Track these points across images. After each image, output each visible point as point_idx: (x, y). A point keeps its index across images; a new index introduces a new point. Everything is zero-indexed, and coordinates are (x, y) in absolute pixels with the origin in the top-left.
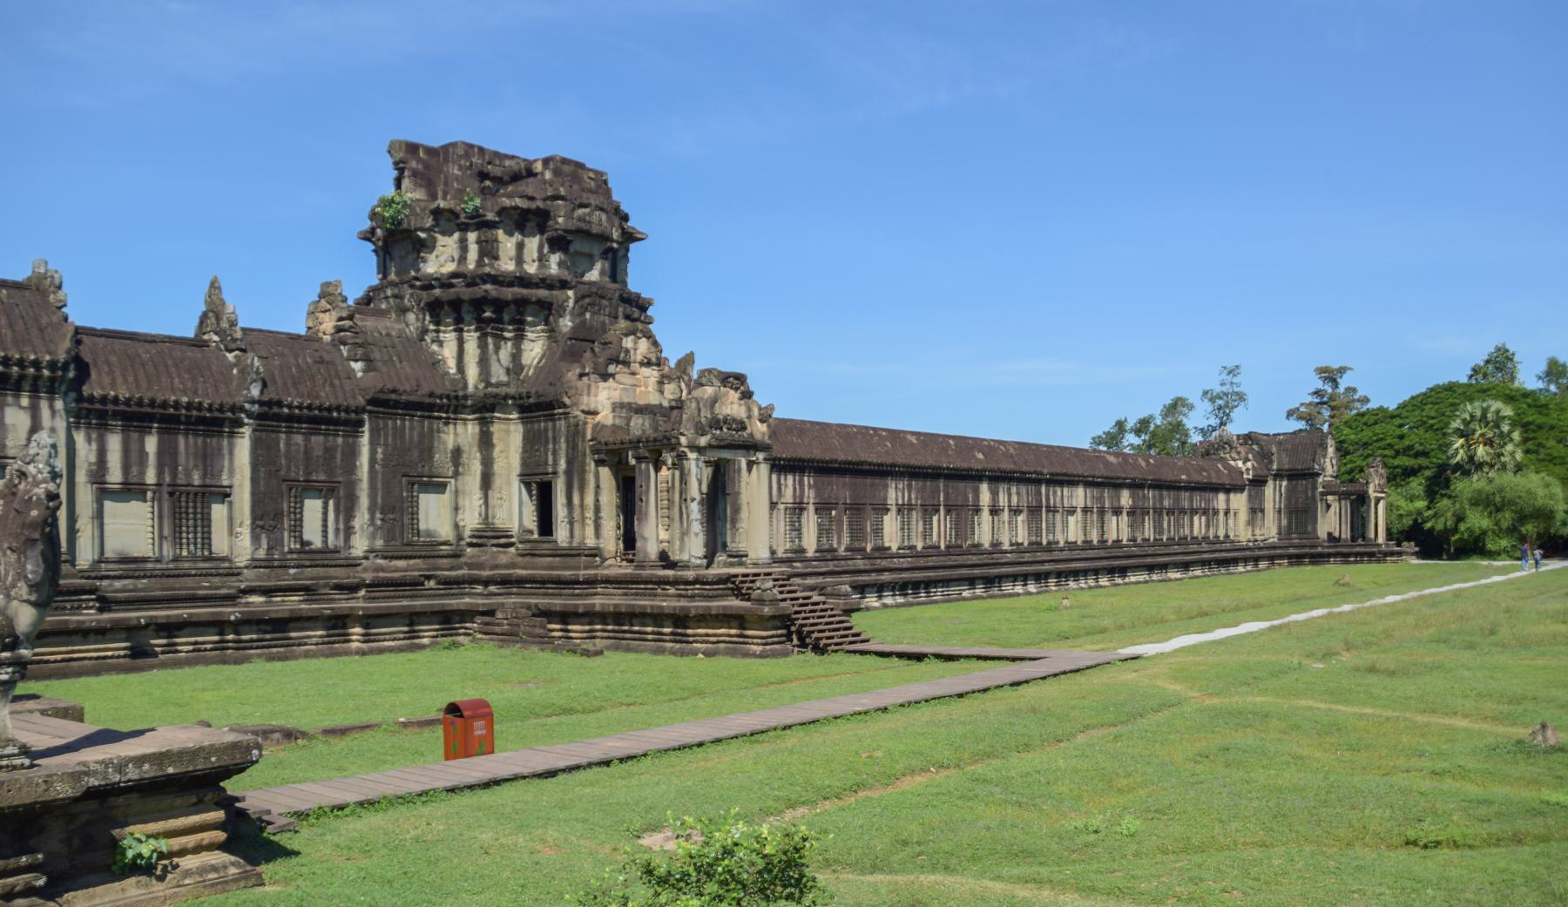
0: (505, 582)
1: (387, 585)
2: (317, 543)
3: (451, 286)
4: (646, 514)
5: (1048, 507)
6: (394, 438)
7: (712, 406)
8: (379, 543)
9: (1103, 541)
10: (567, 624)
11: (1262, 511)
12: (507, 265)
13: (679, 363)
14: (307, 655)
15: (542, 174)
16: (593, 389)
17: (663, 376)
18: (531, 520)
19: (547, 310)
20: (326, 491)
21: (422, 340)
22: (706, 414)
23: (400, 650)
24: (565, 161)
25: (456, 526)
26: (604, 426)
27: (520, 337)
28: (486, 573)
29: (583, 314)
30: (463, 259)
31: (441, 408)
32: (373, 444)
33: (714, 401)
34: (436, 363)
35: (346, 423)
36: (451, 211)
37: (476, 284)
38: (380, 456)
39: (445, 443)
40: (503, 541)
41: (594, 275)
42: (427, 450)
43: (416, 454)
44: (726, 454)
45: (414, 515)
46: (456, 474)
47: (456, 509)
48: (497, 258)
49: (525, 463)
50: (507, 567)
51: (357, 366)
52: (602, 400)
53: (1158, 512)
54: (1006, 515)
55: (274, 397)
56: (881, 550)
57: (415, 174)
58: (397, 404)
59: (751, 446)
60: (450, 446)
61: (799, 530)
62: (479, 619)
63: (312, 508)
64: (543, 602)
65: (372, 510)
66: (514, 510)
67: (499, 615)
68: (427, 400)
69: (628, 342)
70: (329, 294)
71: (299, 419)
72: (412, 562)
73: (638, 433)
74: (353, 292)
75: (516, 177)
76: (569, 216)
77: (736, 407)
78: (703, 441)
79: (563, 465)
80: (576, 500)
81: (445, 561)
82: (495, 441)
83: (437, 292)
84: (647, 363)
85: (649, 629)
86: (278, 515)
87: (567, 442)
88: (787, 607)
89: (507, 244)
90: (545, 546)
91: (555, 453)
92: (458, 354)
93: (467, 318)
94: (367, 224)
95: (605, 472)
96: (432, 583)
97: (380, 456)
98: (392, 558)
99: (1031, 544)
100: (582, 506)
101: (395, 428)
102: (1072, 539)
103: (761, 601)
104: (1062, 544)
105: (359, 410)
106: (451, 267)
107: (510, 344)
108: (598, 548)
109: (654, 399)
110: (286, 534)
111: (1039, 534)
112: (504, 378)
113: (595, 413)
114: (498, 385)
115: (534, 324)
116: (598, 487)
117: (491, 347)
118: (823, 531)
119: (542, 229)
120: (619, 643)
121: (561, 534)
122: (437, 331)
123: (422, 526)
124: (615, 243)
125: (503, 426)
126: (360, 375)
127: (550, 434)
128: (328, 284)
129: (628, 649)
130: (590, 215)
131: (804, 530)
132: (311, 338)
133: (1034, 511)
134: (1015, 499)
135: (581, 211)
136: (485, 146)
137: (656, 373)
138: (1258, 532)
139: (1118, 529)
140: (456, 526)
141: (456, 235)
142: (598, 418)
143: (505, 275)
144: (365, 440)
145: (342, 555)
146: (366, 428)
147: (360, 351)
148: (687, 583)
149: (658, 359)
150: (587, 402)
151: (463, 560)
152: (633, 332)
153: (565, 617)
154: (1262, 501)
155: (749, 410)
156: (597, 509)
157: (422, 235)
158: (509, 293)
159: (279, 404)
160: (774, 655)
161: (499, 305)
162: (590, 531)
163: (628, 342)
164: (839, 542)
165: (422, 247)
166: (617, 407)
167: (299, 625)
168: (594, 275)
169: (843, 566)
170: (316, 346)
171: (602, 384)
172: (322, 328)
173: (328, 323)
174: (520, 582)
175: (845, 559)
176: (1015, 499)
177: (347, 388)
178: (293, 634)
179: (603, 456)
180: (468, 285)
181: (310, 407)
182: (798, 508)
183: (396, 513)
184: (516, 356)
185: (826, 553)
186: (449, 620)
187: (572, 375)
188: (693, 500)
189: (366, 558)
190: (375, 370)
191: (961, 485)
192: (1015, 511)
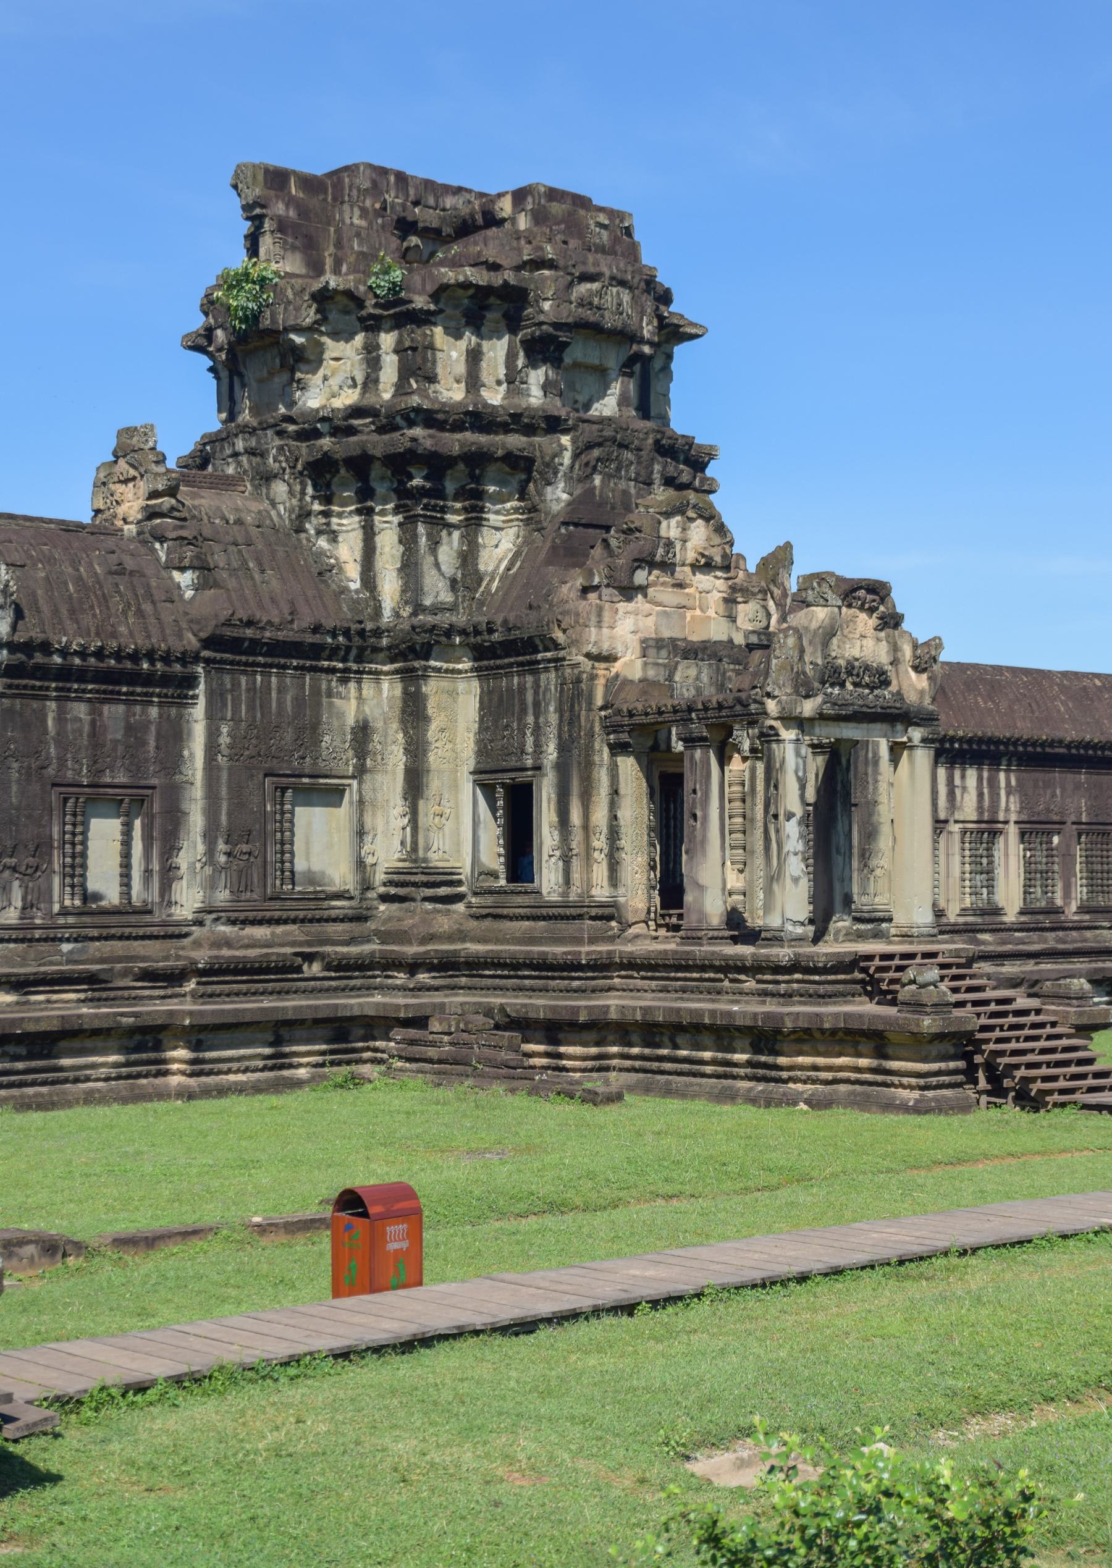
0: (446, 965)
1: (236, 972)
2: (112, 896)
3: (351, 431)
4: (704, 841)
6: (251, 708)
7: (826, 644)
8: (222, 896)
10: (558, 1043)
12: (451, 392)
13: (764, 563)
14: (89, 1099)
15: (513, 220)
16: (607, 616)
17: (733, 589)
19: (524, 471)
20: (129, 803)
21: (300, 530)
22: (813, 656)
23: (257, 1089)
24: (554, 194)
25: (360, 864)
26: (627, 682)
27: (474, 521)
28: (412, 950)
29: (589, 477)
30: (371, 382)
31: (333, 653)
32: (213, 717)
33: (829, 633)
34: (326, 571)
35: (166, 680)
36: (349, 294)
37: (396, 428)
38: (224, 740)
39: (341, 715)
40: (443, 891)
41: (607, 406)
43: (289, 735)
44: (850, 732)
45: (285, 846)
46: (361, 772)
47: (361, 833)
48: (432, 379)
49: (482, 751)
50: (450, 938)
51: (185, 579)
52: (623, 635)
55: (37, 635)
57: (282, 227)
58: (255, 647)
59: (898, 716)
60: (351, 721)
61: (989, 872)
62: (398, 1034)
63: (104, 833)
64: (514, 1002)
66: (464, 834)
67: (435, 1026)
68: (310, 639)
69: (671, 528)
70: (131, 450)
71: (82, 676)
72: (280, 929)
73: (689, 694)
74: (176, 444)
75: (465, 229)
76: (562, 297)
77: (869, 643)
78: (808, 708)
81: (340, 927)
82: (430, 711)
83: (326, 442)
84: (705, 566)
85: (707, 1055)
86: (43, 848)
87: (560, 710)
88: (967, 1018)
89: (451, 352)
90: (520, 900)
91: (537, 730)
92: (364, 555)
93: (381, 489)
94: (198, 321)
95: (628, 765)
96: (316, 968)
97: (224, 740)
98: (245, 922)
100: (586, 827)
101: (252, 689)
103: (917, 1006)
105: (188, 658)
106: (349, 398)
107: (456, 534)
108: (614, 905)
109: (717, 631)
110: (56, 880)
112: (447, 597)
113: (610, 658)
114: (436, 609)
115: (500, 499)
117: (423, 540)
118: (1033, 874)
119: (513, 324)
120: (653, 1078)
121: (548, 878)
122: (326, 514)
123: (300, 865)
124: (646, 351)
125: (445, 684)
126: (189, 594)
127: (530, 697)
128: (130, 431)
129: (668, 1092)
130: (599, 294)
131: (999, 872)
132: (101, 529)
135: (584, 288)
136: (409, 172)
137: (721, 584)
140: (360, 864)
141: (359, 339)
142: (617, 667)
143: (447, 409)
144: (198, 711)
145: (156, 918)
146: (201, 689)
147: (189, 553)
148: (777, 969)
149: (725, 556)
150: (596, 638)
151: (371, 925)
152: (679, 510)
153: (555, 1030)
155: (895, 648)
156: (614, 834)
157: (299, 340)
158: (455, 442)
159: (46, 647)
160: (941, 1108)
161: (437, 465)
162: (600, 872)
163: (671, 528)
165: (297, 361)
166: (650, 646)
167: (76, 1044)
168: (607, 406)
169: (1074, 940)
170: (110, 542)
171: (623, 606)
172: (121, 510)
173: (131, 503)
174: (474, 965)
177: (168, 619)
178: (66, 1062)
179: (625, 737)
180: (381, 430)
181: (99, 654)
182: (987, 831)
183: (253, 843)
184: (468, 557)
185: (1041, 916)
186: (344, 1035)
187: (568, 590)
188: (790, 816)
189: (200, 923)
190: (216, 585)
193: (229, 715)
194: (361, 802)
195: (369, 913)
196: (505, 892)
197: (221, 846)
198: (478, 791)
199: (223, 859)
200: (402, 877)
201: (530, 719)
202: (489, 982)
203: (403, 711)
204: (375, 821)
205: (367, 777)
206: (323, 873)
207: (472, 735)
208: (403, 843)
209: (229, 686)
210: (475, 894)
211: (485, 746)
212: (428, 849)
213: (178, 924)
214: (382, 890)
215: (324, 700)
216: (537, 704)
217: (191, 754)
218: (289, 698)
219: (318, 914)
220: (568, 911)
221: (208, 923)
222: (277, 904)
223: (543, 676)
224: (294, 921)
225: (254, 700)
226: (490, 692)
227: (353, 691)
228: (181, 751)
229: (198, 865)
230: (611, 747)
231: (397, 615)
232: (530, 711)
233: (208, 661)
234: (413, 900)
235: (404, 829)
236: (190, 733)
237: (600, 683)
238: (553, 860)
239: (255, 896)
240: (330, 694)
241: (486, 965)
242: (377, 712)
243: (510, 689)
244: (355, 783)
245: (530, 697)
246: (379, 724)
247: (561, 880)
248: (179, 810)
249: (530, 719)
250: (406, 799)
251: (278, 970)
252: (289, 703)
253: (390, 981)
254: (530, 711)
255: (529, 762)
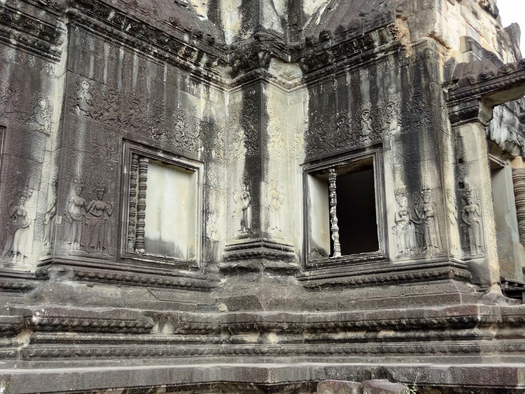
8: (71, 249)
18: (323, 230)
25: (205, 240)
38: (84, 95)
39: (193, 109)
42: (166, 111)
43: (148, 110)
46: (207, 160)
49: (313, 142)
60: (200, 115)
65: (59, 185)
72: (131, 290)
79: (394, 127)
80: (428, 178)
82: (269, 111)
87: (404, 90)
90: (361, 268)
96: (167, 332)
97: (84, 95)
116: (460, 161)
121: (397, 243)
123: (151, 232)
127: (365, 87)
140: (205, 240)
151: (213, 295)
156: (463, 200)
183: (109, 204)
193: (91, 74)
194: (207, 185)
195: (211, 284)
196: (344, 263)
197: (73, 196)
198: (309, 179)
199: (74, 210)
200: (243, 252)
201: (367, 105)
202: (340, 347)
203: (244, 113)
204: (218, 203)
205: (212, 165)
206: (173, 244)
207: (302, 136)
208: (243, 223)
209: (92, 48)
210: (308, 268)
211: (317, 139)
212: (267, 225)
213: (17, 276)
214: (223, 265)
215: (179, 91)
216: (374, 93)
217: (49, 107)
218: (149, 79)
219: (168, 280)
220: (427, 272)
221: (52, 276)
222: (128, 265)
223: (380, 68)
224: (145, 284)
225: (116, 70)
226: (320, 96)
227: (202, 91)
228: (38, 99)
229: (48, 217)
230: (453, 119)
231: (238, 39)
232: (367, 98)
233: (70, 15)
234: (256, 270)
235: (244, 210)
236: (49, 86)
237: (441, 63)
238: (401, 225)
239: (106, 255)
240: (184, 89)
241: (335, 329)
242: (221, 115)
243: (343, 89)
244: (202, 167)
245: (365, 87)
246: (223, 125)
247: (412, 242)
248: (30, 157)
249: (367, 105)
250: (246, 184)
251: (129, 330)
252: (148, 83)
253: (237, 347)
254: (367, 98)
255: (368, 142)
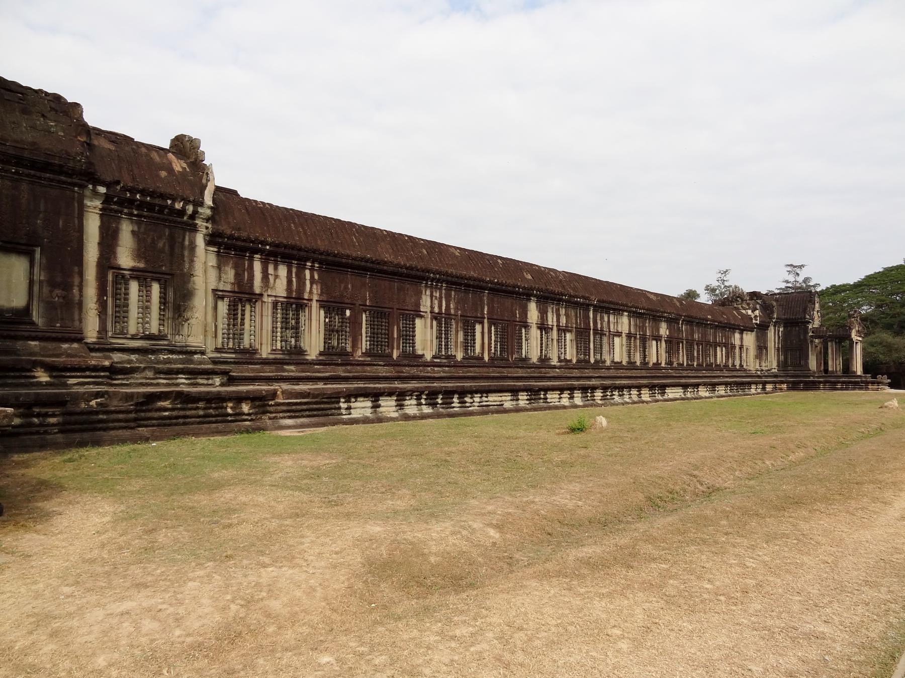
5: (595, 330)
9: (645, 363)
11: (766, 348)
53: (690, 343)
54: (555, 334)
56: (413, 358)
99: (578, 361)
102: (617, 359)
104: (608, 363)
111: (587, 352)
133: (582, 335)
134: (563, 320)
138: (763, 364)
139: (656, 353)
154: (765, 341)
164: (354, 346)
175: (362, 364)
176: (563, 320)
191: (508, 302)
192: (562, 330)
